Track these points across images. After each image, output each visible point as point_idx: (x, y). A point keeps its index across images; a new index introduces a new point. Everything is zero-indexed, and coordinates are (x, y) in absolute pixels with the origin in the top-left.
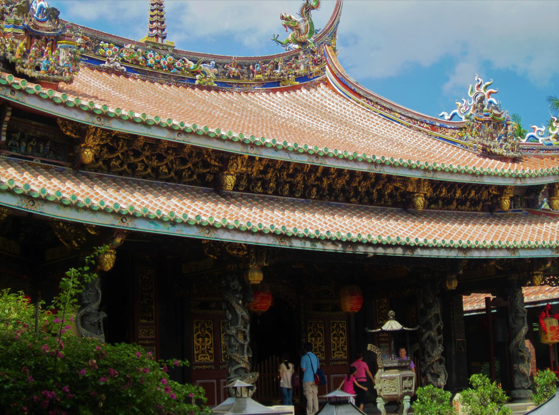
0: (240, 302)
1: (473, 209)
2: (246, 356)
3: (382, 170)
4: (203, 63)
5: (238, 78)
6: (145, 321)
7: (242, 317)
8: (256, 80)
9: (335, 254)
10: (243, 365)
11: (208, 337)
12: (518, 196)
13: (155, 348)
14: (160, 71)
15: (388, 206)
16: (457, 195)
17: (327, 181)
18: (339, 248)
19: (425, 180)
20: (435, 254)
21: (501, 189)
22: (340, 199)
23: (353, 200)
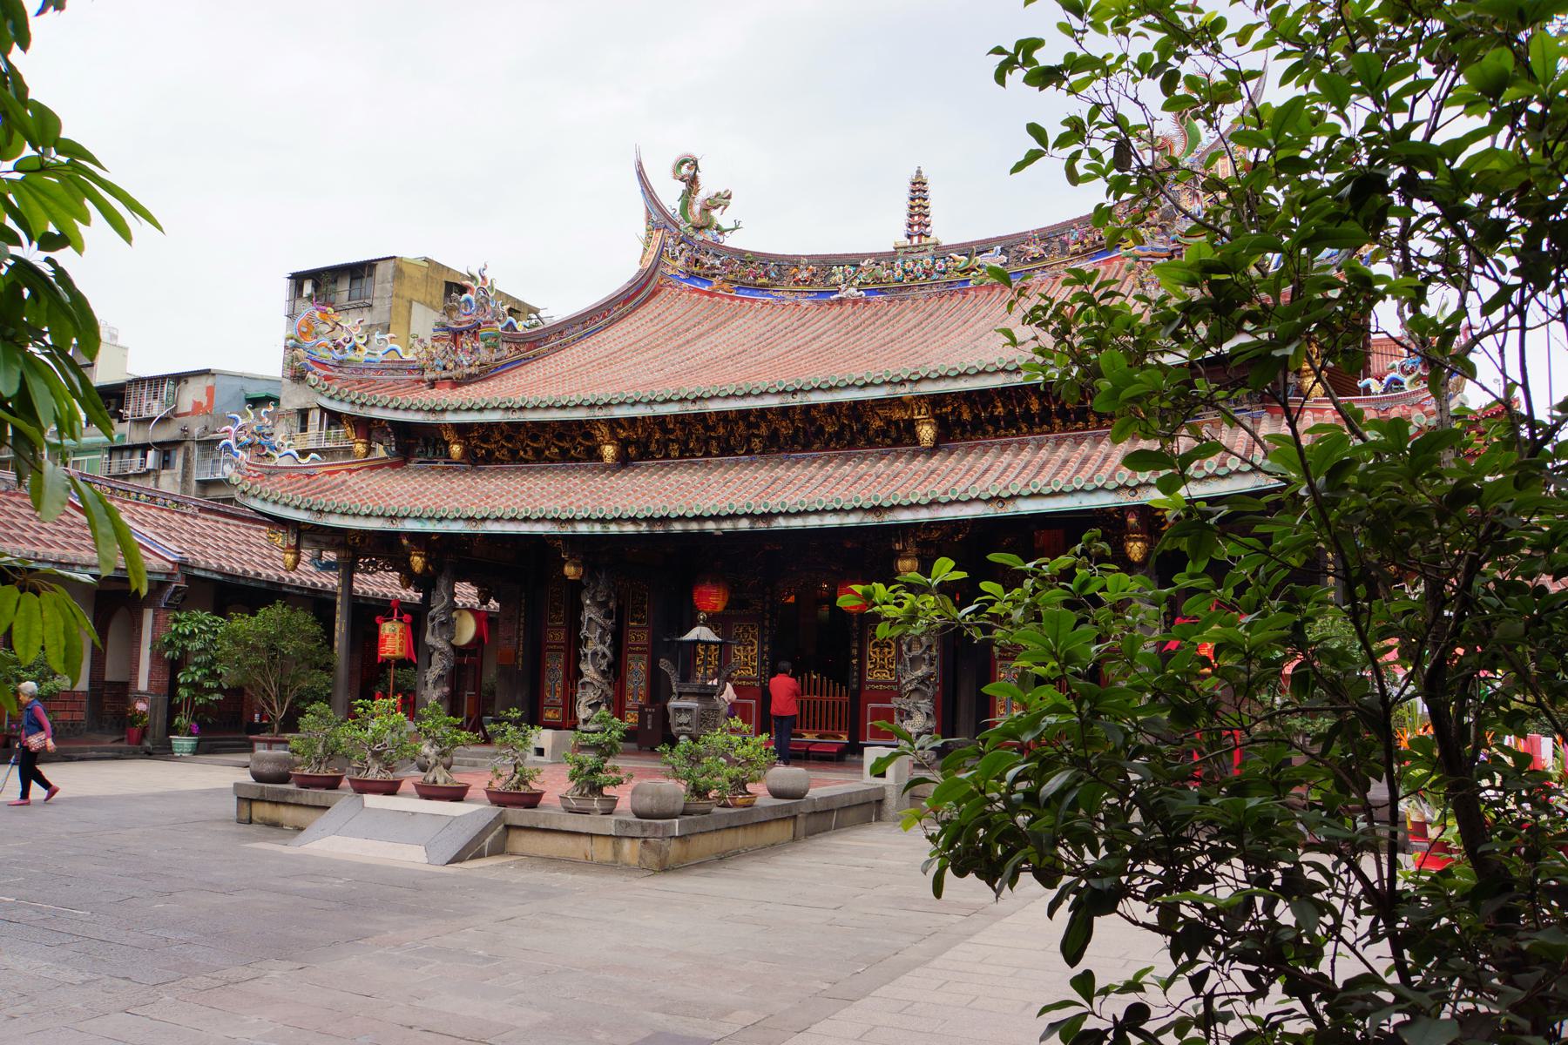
2: (591, 667)
3: (805, 399)
4: (979, 253)
5: (1042, 257)
7: (590, 619)
8: (1073, 254)
9: (638, 537)
10: (587, 679)
11: (752, 644)
13: (646, 656)
14: (916, 283)
15: (907, 445)
16: (1035, 407)
17: (768, 427)
18: (644, 528)
20: (813, 522)
22: (815, 447)
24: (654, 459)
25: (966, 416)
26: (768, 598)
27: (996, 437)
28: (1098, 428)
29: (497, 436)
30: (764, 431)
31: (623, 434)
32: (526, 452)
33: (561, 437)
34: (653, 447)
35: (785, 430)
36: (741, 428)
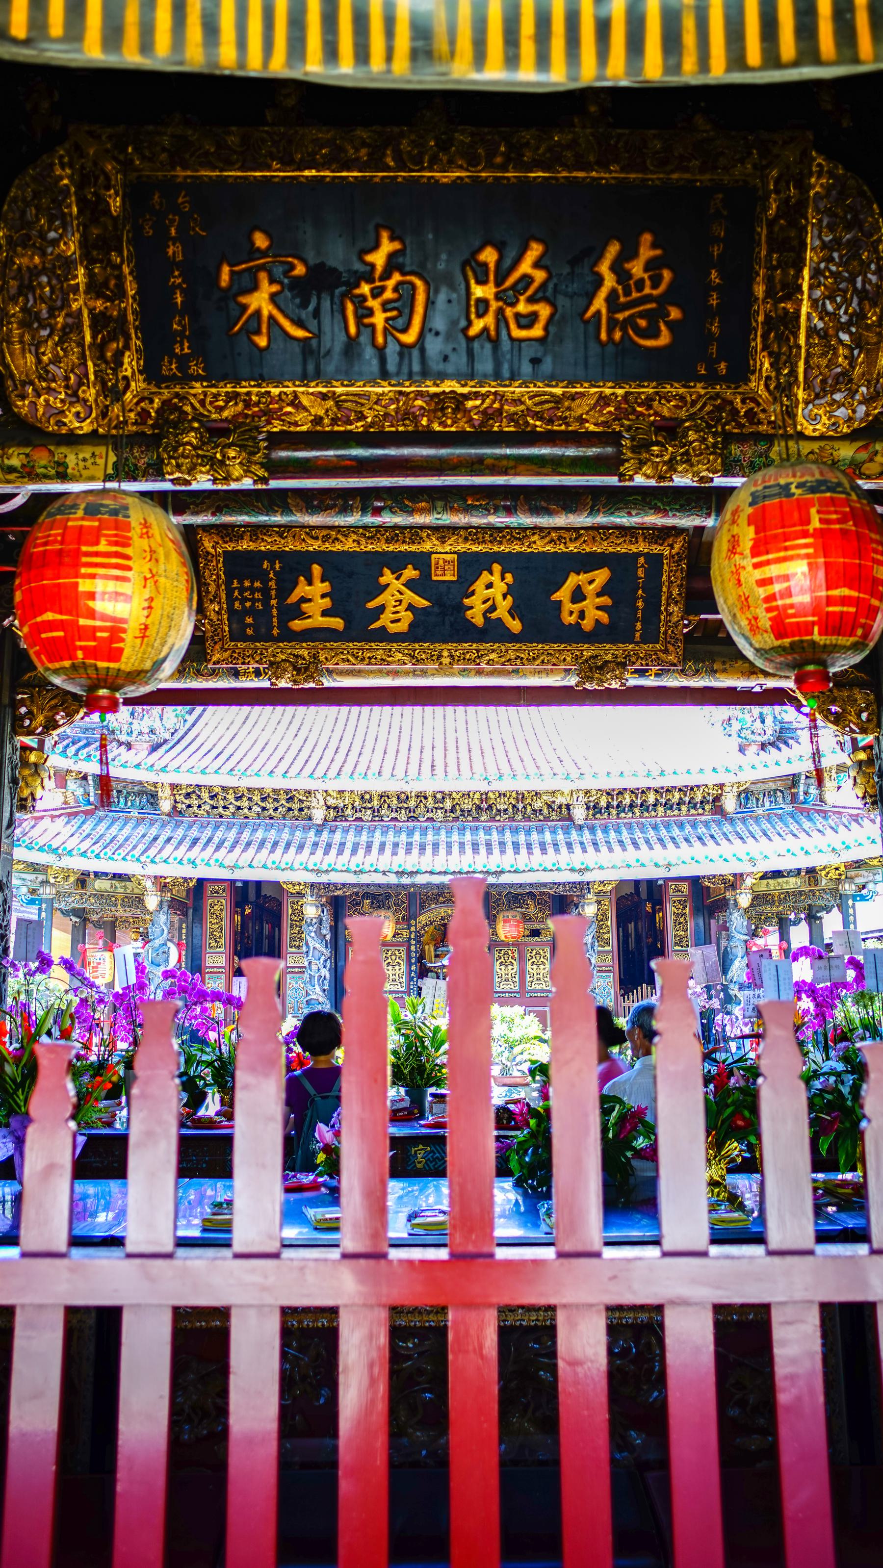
0: (313, 934)
1: (693, 811)
2: (317, 987)
6: (294, 950)
12: (775, 791)
18: (393, 879)
19: (578, 791)
21: (721, 786)
22: (482, 819)
23: (498, 818)
24: (346, 820)
25: (603, 803)
26: (413, 929)
27: (618, 818)
28: (688, 815)
29: (205, 796)
30: (448, 804)
31: (331, 802)
32: (225, 808)
33: (263, 799)
34: (349, 812)
35: (467, 805)
36: (430, 802)
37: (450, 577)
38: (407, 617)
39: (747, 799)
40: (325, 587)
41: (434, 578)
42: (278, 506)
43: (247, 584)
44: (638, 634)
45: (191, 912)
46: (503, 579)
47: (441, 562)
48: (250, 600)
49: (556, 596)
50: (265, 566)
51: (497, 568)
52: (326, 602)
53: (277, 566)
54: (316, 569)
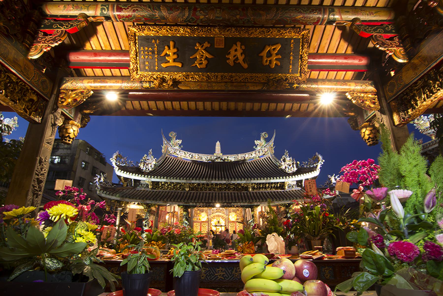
16: (267, 185)
34: (195, 189)
37: (222, 46)
38: (205, 62)
39: (290, 186)
40: (175, 50)
41: (216, 47)
42: (156, 10)
43: (146, 49)
44: (290, 70)
45: (156, 214)
46: (241, 48)
47: (218, 41)
48: (147, 55)
49: (261, 55)
50: (153, 42)
51: (239, 44)
52: (175, 57)
53: (158, 41)
54: (172, 44)
